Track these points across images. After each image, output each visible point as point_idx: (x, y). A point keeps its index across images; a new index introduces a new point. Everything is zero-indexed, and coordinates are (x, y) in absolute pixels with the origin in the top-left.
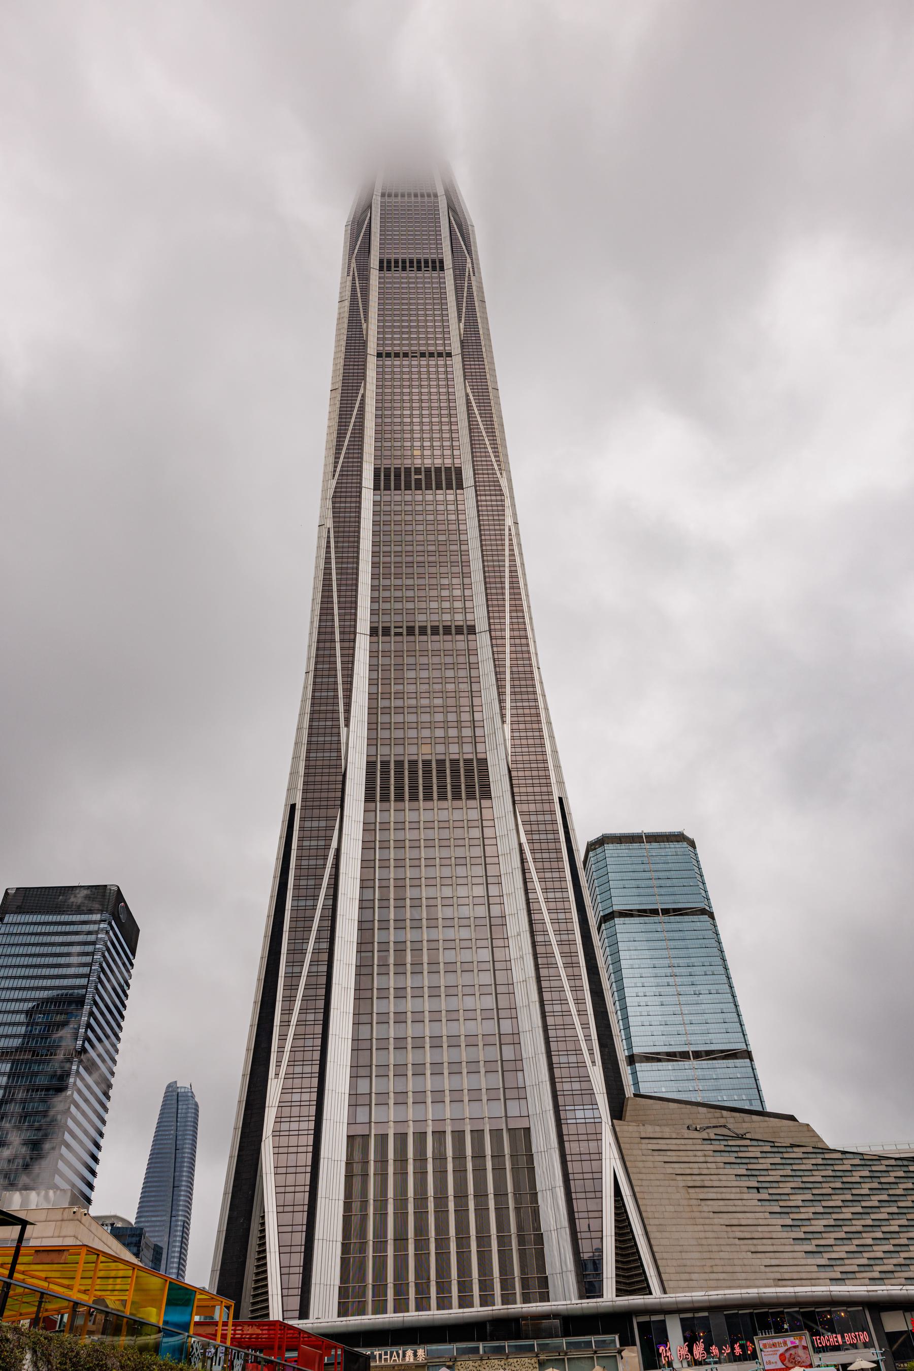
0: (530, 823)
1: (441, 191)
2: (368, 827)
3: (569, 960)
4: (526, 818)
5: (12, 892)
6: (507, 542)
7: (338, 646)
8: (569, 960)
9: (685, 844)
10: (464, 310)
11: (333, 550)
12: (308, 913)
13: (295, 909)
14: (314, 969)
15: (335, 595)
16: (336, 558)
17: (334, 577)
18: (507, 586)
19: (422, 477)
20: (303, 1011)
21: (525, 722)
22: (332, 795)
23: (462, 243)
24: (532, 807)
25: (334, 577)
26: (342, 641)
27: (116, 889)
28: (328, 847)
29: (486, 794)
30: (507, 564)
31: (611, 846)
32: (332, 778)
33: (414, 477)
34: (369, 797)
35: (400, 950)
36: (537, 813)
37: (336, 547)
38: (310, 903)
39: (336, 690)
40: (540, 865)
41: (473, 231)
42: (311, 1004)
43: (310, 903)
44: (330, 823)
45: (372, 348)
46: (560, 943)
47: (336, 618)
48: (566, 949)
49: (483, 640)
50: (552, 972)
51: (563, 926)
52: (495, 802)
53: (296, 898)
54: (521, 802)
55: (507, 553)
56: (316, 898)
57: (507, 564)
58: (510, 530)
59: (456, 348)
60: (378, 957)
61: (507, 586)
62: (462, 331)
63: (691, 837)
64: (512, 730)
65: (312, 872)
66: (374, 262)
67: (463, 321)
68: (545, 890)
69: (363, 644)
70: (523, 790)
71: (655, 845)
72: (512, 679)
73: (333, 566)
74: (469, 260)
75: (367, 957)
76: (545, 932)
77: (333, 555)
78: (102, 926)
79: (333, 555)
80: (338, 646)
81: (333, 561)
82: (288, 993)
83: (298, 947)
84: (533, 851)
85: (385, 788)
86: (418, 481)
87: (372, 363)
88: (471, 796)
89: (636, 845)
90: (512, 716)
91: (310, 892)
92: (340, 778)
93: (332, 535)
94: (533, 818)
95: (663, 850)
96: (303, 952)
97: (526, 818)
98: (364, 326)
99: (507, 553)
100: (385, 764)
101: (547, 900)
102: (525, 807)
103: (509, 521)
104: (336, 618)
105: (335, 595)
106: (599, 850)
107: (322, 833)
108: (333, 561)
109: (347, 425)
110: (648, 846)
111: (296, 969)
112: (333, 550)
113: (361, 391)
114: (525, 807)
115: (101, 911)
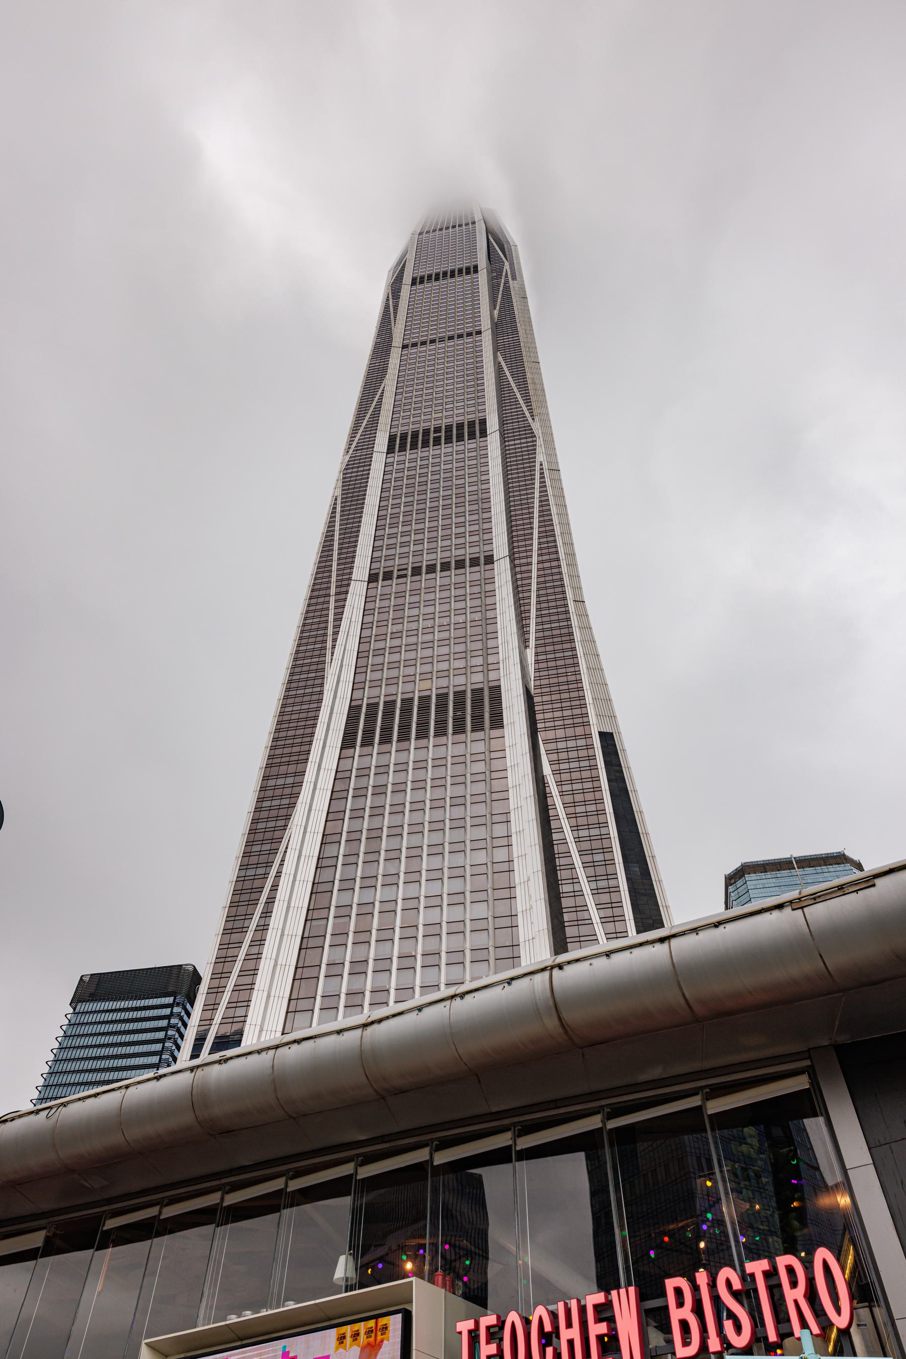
0: (557, 751)
1: (478, 217)
2: (341, 776)
3: (609, 912)
4: (552, 746)
5: (87, 979)
6: (537, 476)
8: (609, 912)
9: (848, 866)
10: (499, 300)
12: (257, 884)
15: (335, 553)
17: (336, 537)
18: (536, 515)
21: (553, 644)
23: (501, 253)
24: (560, 733)
25: (336, 537)
27: (191, 969)
29: (497, 721)
30: (537, 495)
31: (753, 876)
34: (348, 742)
35: (366, 912)
36: (566, 739)
38: (261, 871)
40: (569, 799)
41: (516, 250)
43: (261, 871)
46: (596, 892)
47: (334, 574)
48: (605, 898)
50: (584, 930)
51: (601, 870)
52: (507, 731)
54: (546, 729)
55: (537, 485)
57: (537, 495)
58: (541, 465)
60: (334, 924)
61: (536, 515)
62: (496, 316)
63: (855, 858)
64: (537, 654)
65: (268, 835)
66: (407, 279)
67: (498, 308)
68: (575, 828)
70: (548, 715)
71: (809, 870)
72: (538, 603)
73: (337, 528)
74: (507, 264)
75: (319, 926)
76: (574, 880)
77: (338, 518)
78: (176, 1010)
79: (338, 518)
82: (216, 983)
83: (238, 924)
84: (559, 783)
88: (478, 726)
89: (785, 873)
90: (537, 639)
91: (263, 859)
93: (339, 501)
94: (561, 745)
95: (820, 876)
97: (552, 746)
99: (537, 485)
100: (373, 707)
101: (578, 840)
102: (551, 735)
103: (540, 457)
104: (334, 574)
105: (335, 553)
106: (739, 883)
107: (287, 791)
109: (367, 410)
110: (799, 872)
111: (231, 952)
114: (551, 735)
115: (173, 994)
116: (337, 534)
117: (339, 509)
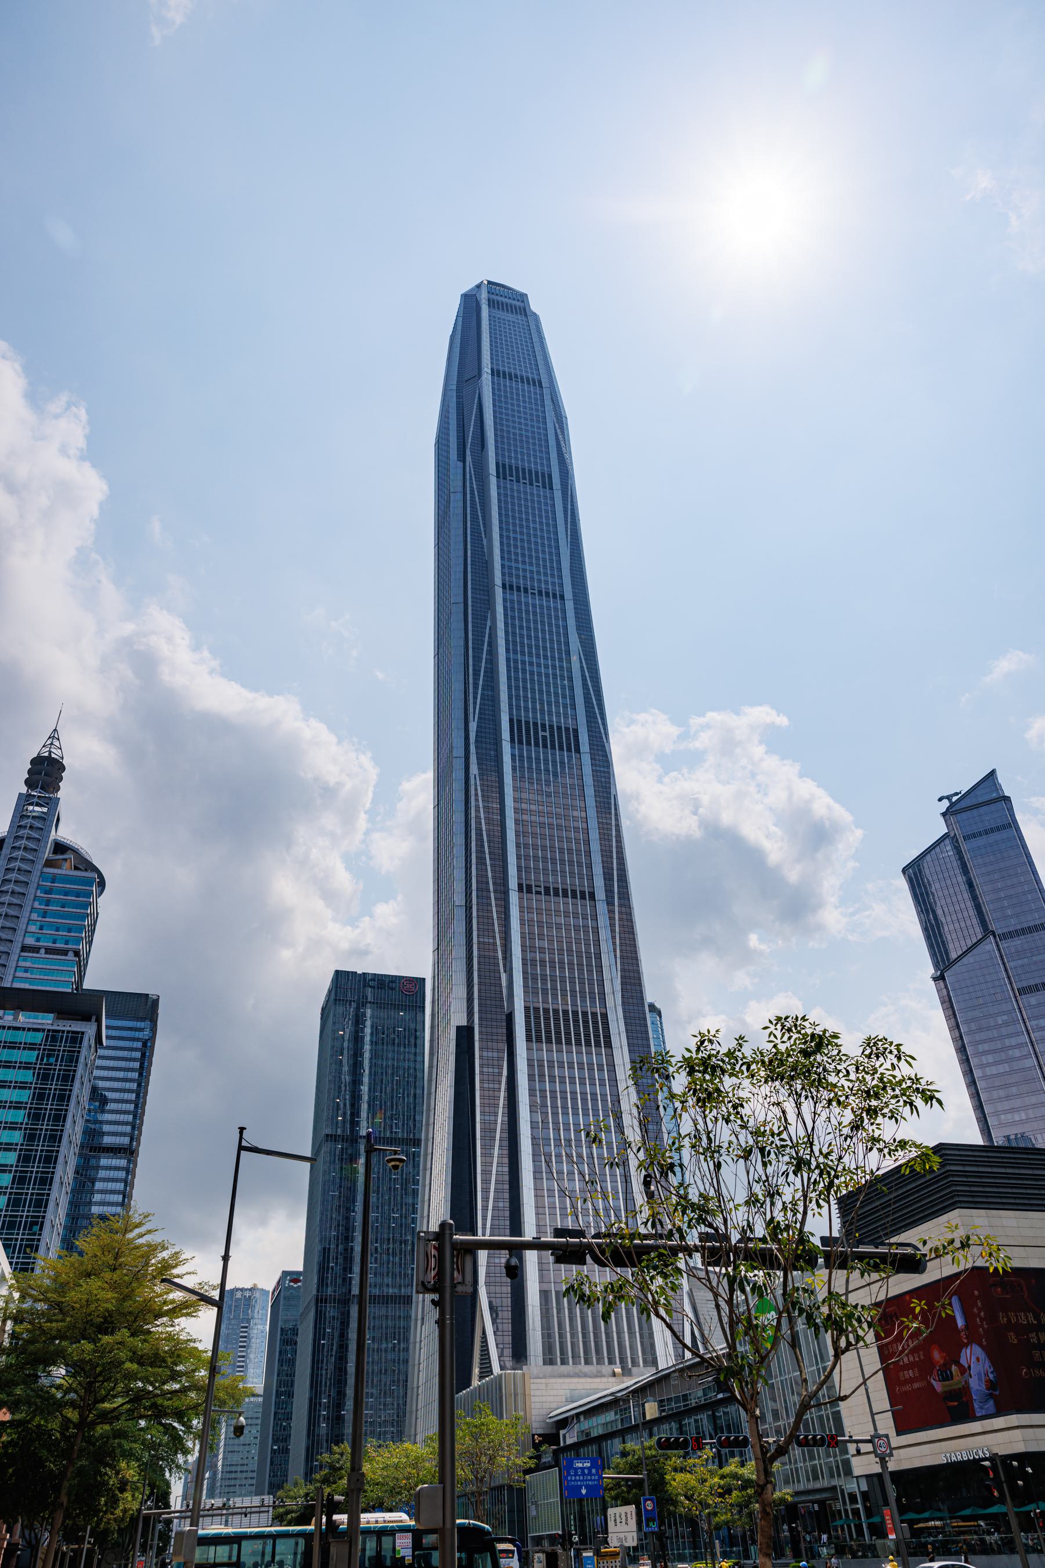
7: (492, 895)
11: (480, 799)
13: (483, 1122)
14: (500, 1169)
16: (484, 807)
19: (547, 734)
20: (496, 1200)
22: (500, 1031)
26: (495, 891)
28: (500, 1074)
32: (499, 1017)
33: (541, 733)
37: (483, 796)
39: (494, 937)
42: (500, 1195)
44: (500, 1055)
45: (498, 581)
49: (602, 908)
53: (483, 1113)
56: (496, 1114)
59: (568, 594)
69: (514, 897)
79: (481, 805)
80: (492, 895)
81: (482, 810)
85: (538, 1031)
86: (544, 738)
87: (499, 592)
92: (504, 1017)
96: (491, 1156)
98: (485, 542)
108: (482, 810)
112: (480, 799)
113: (489, 624)
116: (483, 821)
117: (480, 793)
